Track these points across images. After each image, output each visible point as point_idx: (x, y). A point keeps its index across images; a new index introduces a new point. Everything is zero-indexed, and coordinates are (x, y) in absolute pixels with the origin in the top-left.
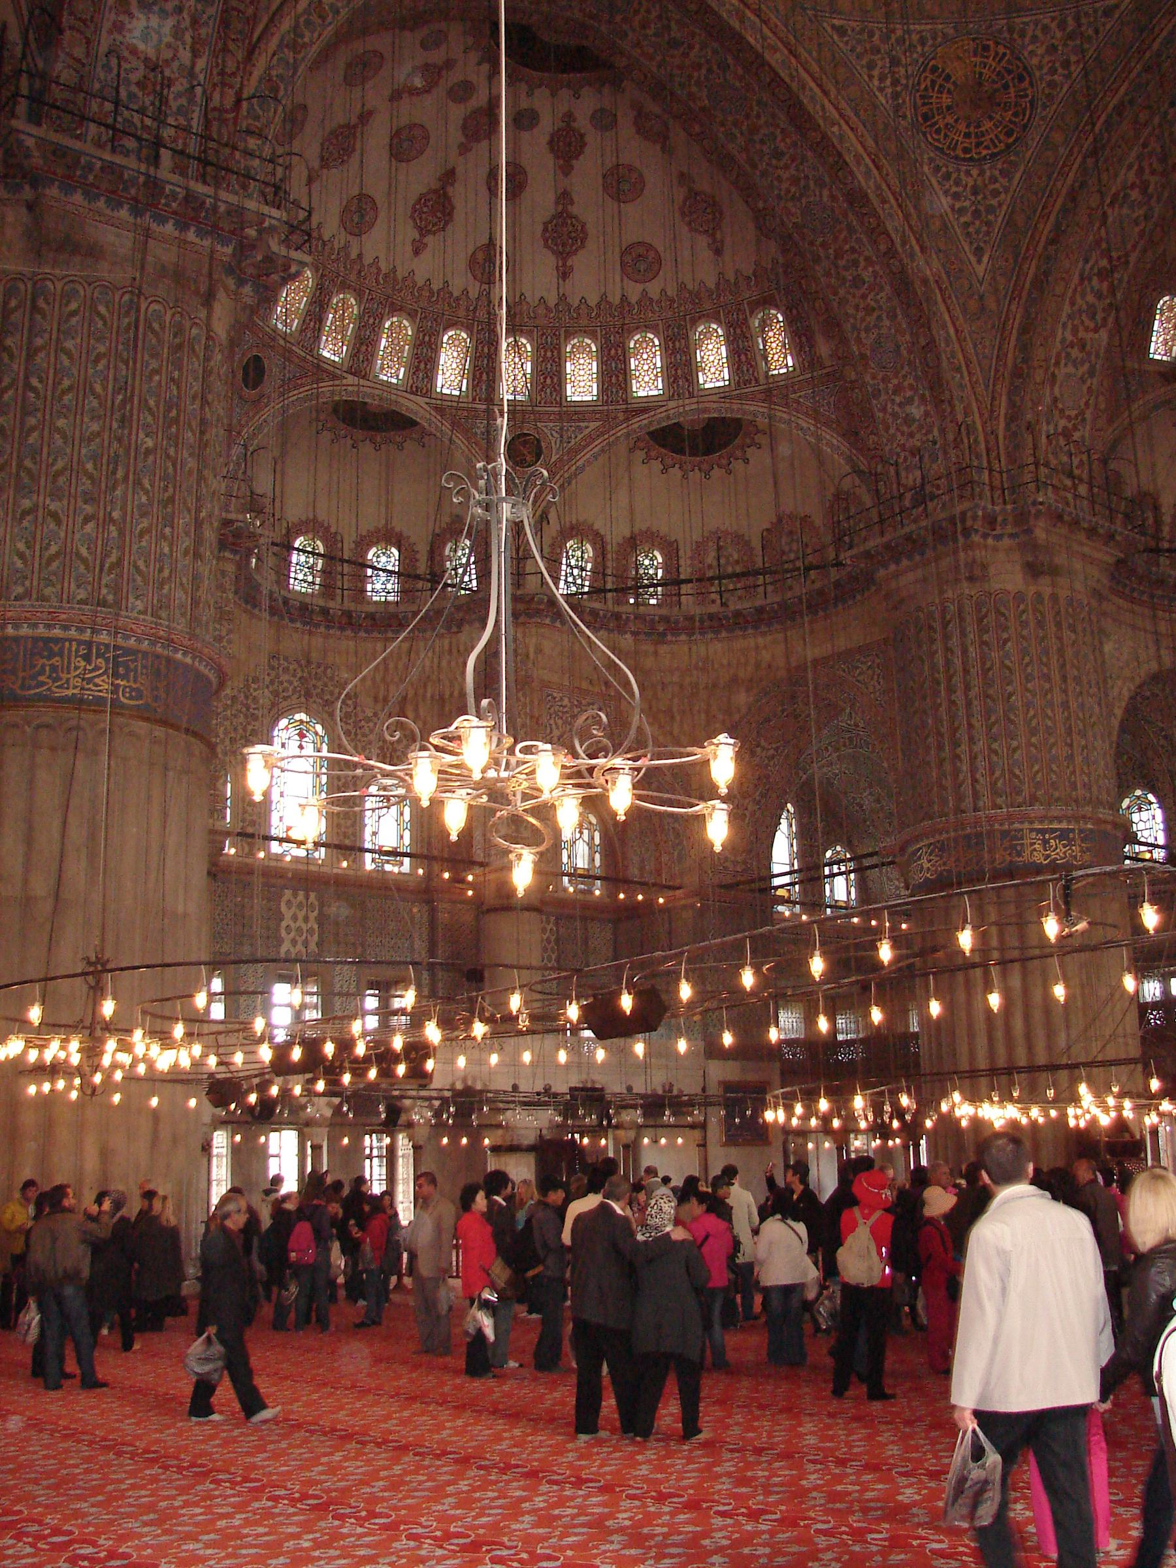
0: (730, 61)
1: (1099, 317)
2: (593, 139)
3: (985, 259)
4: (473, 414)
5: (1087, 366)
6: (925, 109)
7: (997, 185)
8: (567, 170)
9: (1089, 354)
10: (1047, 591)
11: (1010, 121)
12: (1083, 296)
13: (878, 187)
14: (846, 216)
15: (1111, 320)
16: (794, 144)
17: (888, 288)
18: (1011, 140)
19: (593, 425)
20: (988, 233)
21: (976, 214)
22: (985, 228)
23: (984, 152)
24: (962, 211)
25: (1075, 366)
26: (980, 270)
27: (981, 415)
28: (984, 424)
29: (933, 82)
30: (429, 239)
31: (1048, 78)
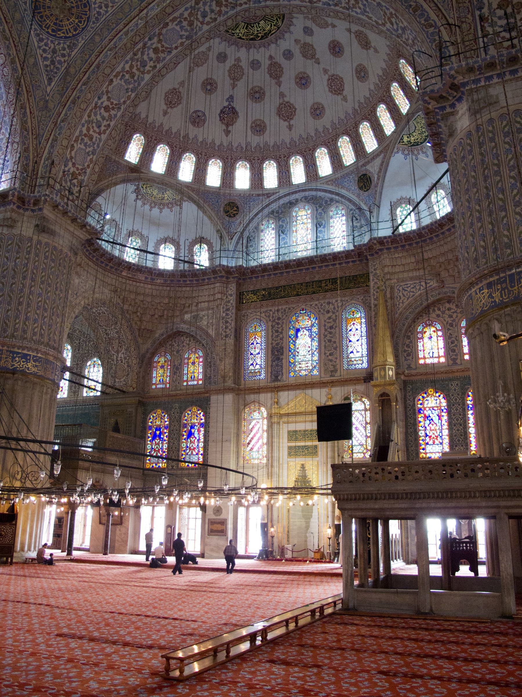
5: (92, 148)
7: (65, 52)
9: (94, 144)
11: (77, 24)
12: (95, 115)
15: (108, 132)
18: (74, 33)
20: (56, 73)
21: (53, 62)
22: (55, 70)
23: (62, 35)
24: (46, 59)
25: (85, 145)
26: (49, 89)
28: (34, 158)
31: (98, 10)
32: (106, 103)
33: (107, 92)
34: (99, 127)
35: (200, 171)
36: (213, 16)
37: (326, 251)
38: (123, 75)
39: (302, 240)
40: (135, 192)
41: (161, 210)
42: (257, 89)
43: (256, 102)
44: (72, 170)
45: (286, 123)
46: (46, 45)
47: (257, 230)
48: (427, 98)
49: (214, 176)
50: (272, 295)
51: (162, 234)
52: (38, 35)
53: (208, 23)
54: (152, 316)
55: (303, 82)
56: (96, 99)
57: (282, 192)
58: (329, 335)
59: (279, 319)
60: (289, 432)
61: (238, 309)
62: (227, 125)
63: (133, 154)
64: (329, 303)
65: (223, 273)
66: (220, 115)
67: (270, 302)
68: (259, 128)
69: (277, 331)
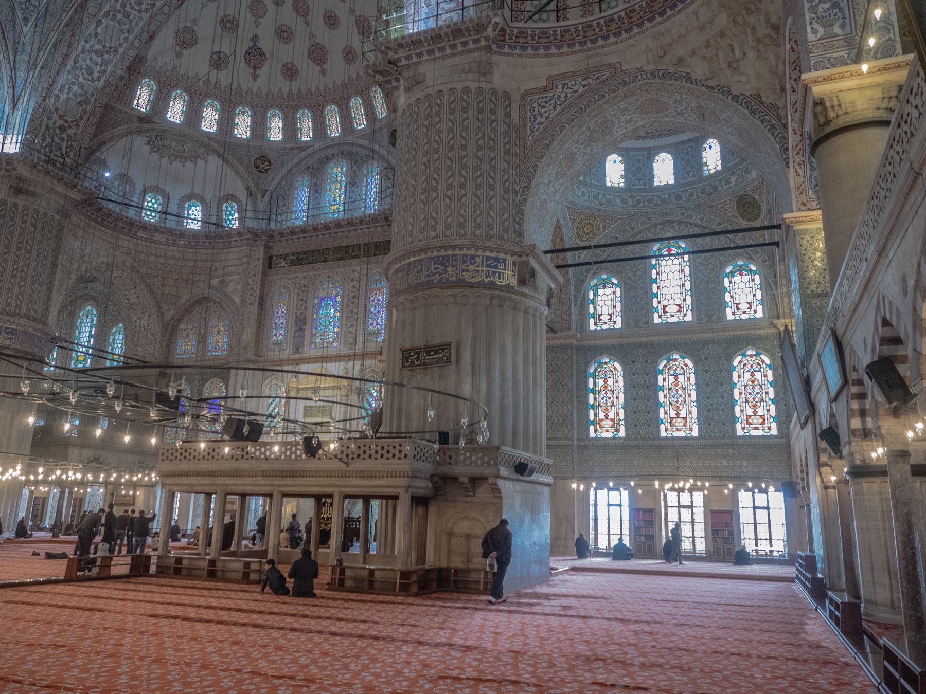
3: (30, 24)
10: (21, 203)
15: (103, 79)
32: (97, 47)
34: (91, 73)
35: (226, 122)
37: (358, 214)
39: (335, 200)
40: (148, 143)
42: (284, 28)
43: (284, 42)
45: (318, 68)
47: (291, 187)
48: (370, 72)
49: (243, 128)
50: (300, 259)
51: (186, 190)
54: (176, 280)
55: (333, 22)
56: (83, 43)
57: (317, 146)
58: (351, 305)
59: (305, 286)
60: (305, 407)
61: (264, 274)
62: (255, 68)
63: (142, 99)
64: (354, 271)
65: (249, 236)
66: (245, 57)
67: (298, 268)
68: (290, 72)
69: (302, 300)
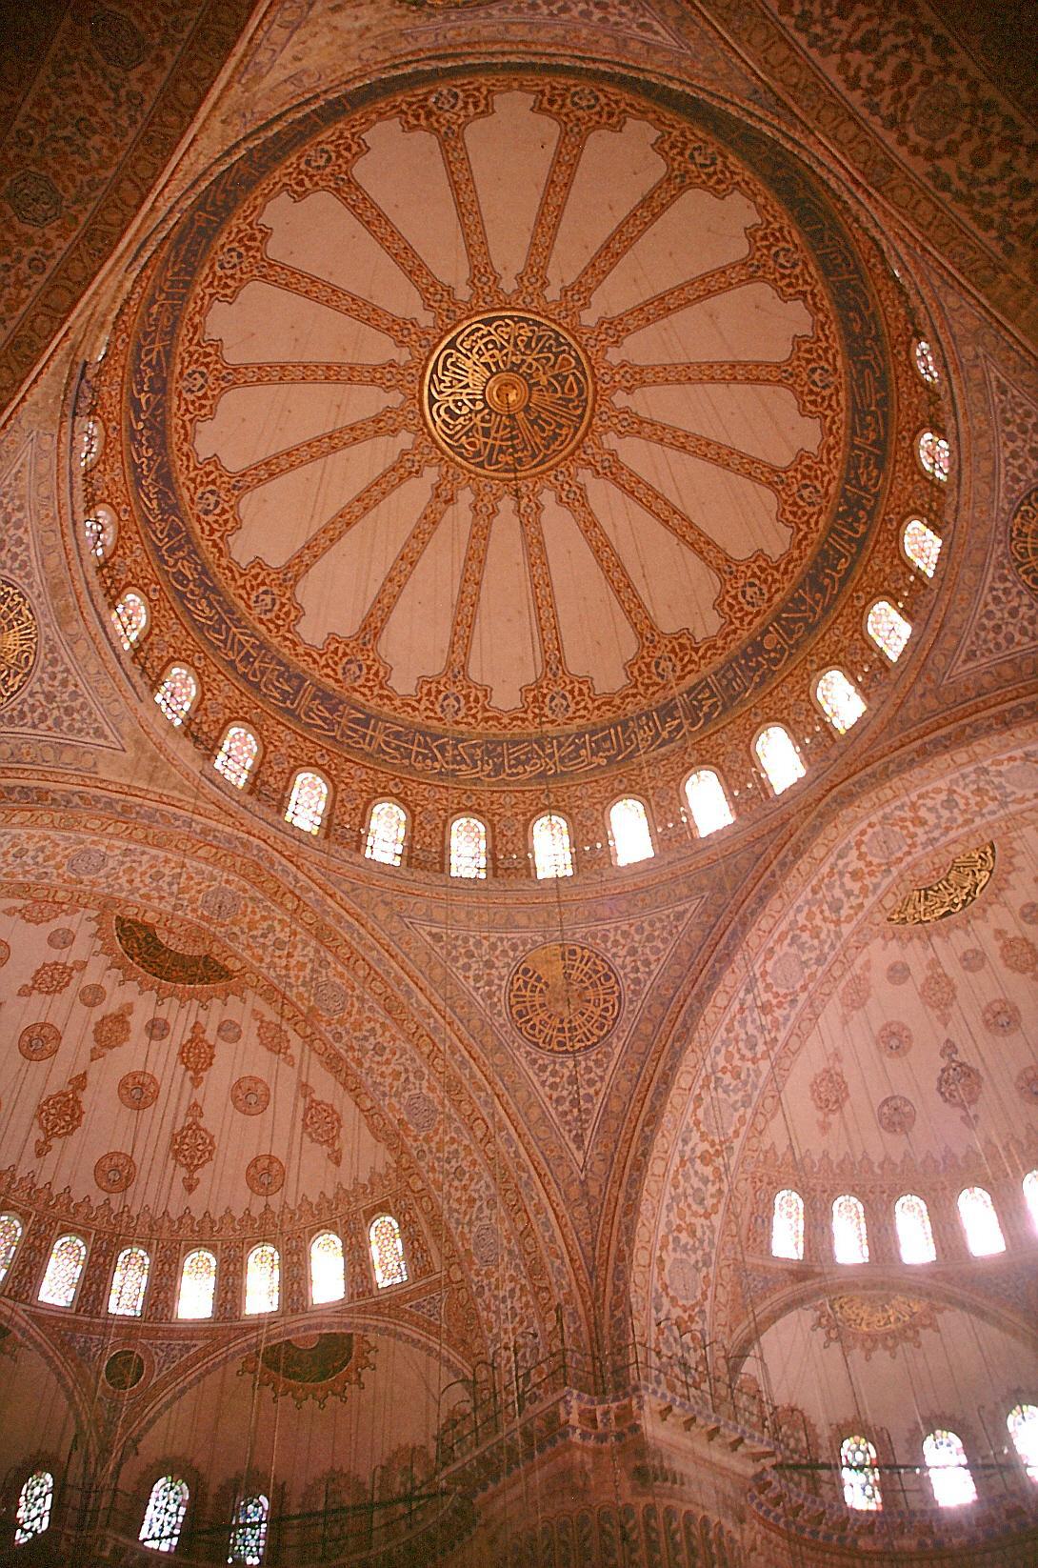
0: (330, 958)
1: (709, 1202)
2: (223, 1050)
4: (76, 1325)
6: (519, 1007)
8: (196, 1082)
9: (701, 1242)
13: (472, 1076)
14: (443, 1105)
15: (721, 1208)
16: (393, 1039)
17: (485, 1174)
19: (201, 1344)
23: (578, 1046)
24: (559, 1101)
27: (584, 1303)
29: (526, 983)
30: (55, 1143)
33: (697, 1123)
34: (701, 1202)
36: (854, 901)
38: (718, 1079)
41: (892, 1350)
42: (997, 1007)
44: (674, 1316)
46: (554, 1073)
52: (534, 1062)
53: (849, 919)
66: (939, 1089)
